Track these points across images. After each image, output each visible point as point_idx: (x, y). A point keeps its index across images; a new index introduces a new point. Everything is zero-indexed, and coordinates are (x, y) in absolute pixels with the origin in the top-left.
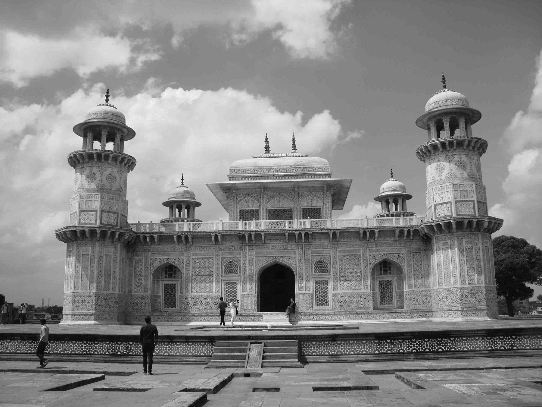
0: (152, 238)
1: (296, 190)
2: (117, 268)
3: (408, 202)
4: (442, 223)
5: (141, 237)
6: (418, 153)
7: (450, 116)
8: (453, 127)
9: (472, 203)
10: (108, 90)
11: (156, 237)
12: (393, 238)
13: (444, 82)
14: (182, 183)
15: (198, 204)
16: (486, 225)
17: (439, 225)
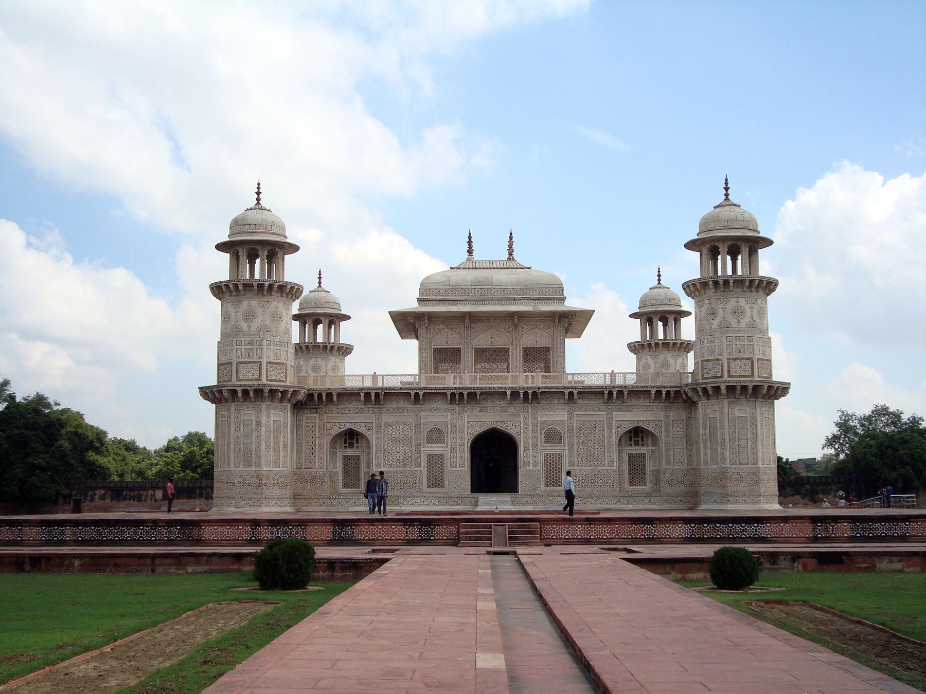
0: (329, 395)
1: (515, 319)
2: (288, 435)
3: (683, 320)
4: (709, 387)
5: (316, 395)
6: (684, 289)
7: (729, 243)
8: (734, 253)
9: (749, 362)
10: (259, 184)
11: (335, 393)
12: (647, 401)
13: (727, 189)
14: (320, 283)
15: (346, 318)
16: (765, 392)
17: (705, 390)
